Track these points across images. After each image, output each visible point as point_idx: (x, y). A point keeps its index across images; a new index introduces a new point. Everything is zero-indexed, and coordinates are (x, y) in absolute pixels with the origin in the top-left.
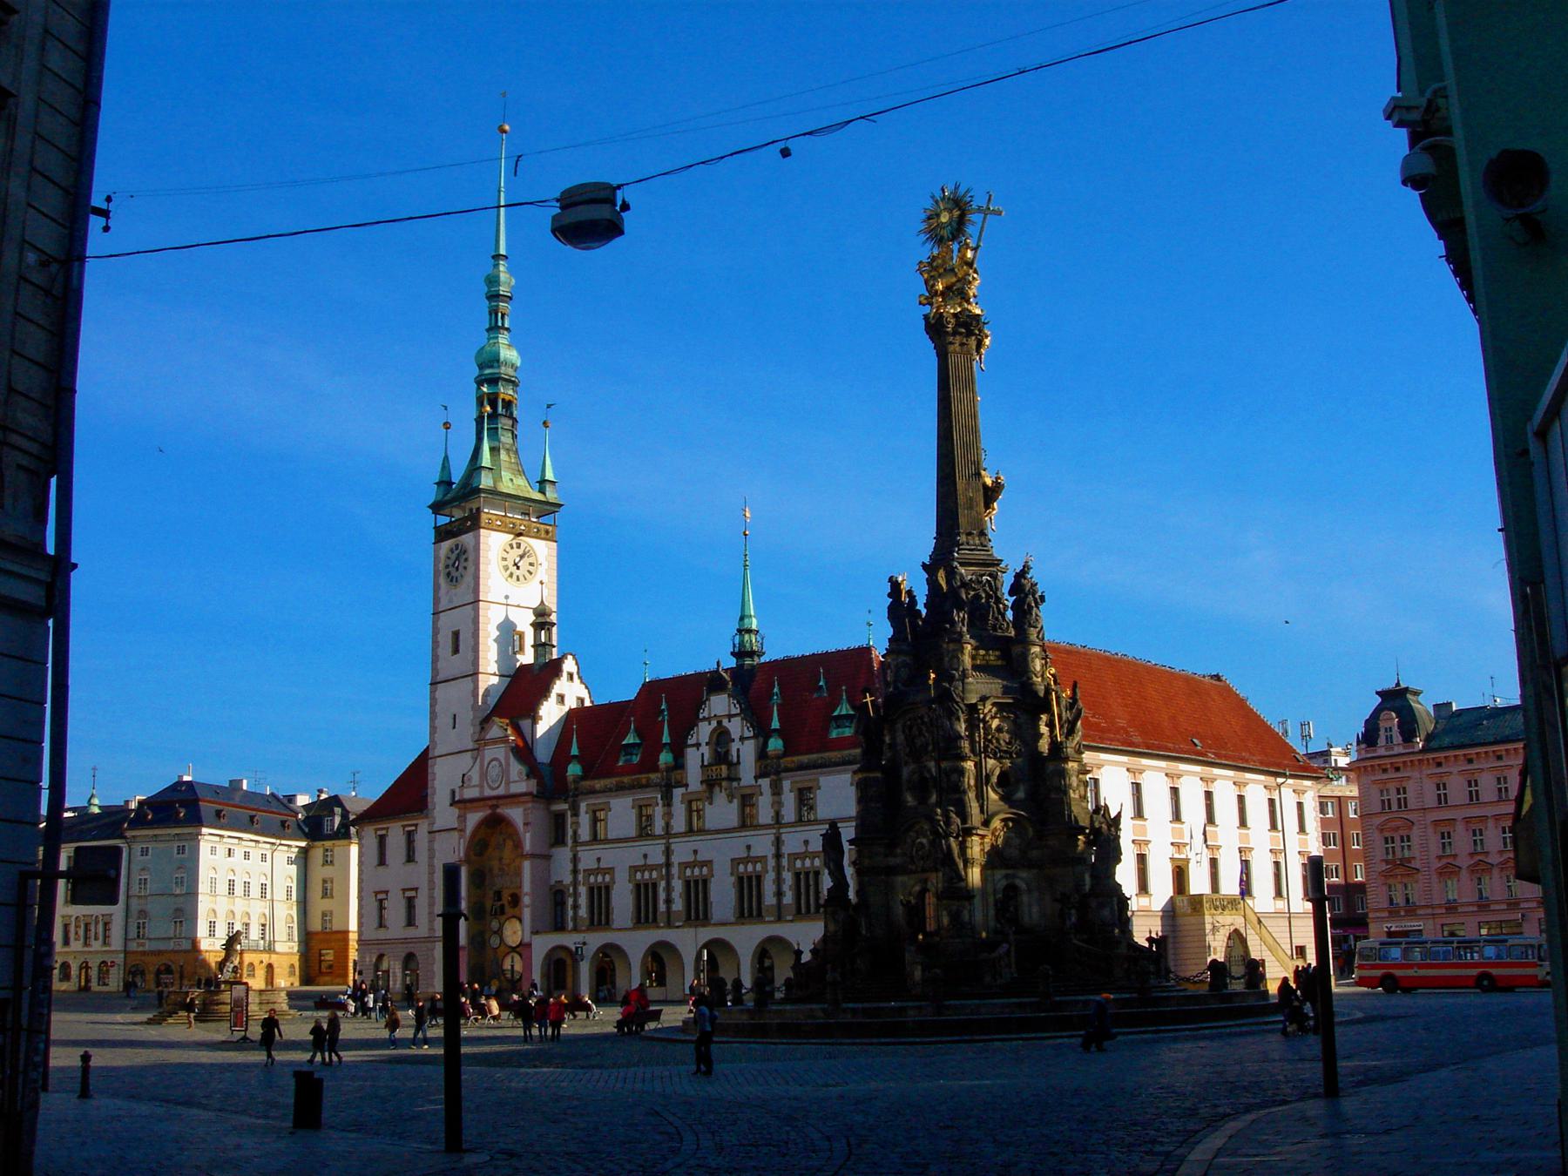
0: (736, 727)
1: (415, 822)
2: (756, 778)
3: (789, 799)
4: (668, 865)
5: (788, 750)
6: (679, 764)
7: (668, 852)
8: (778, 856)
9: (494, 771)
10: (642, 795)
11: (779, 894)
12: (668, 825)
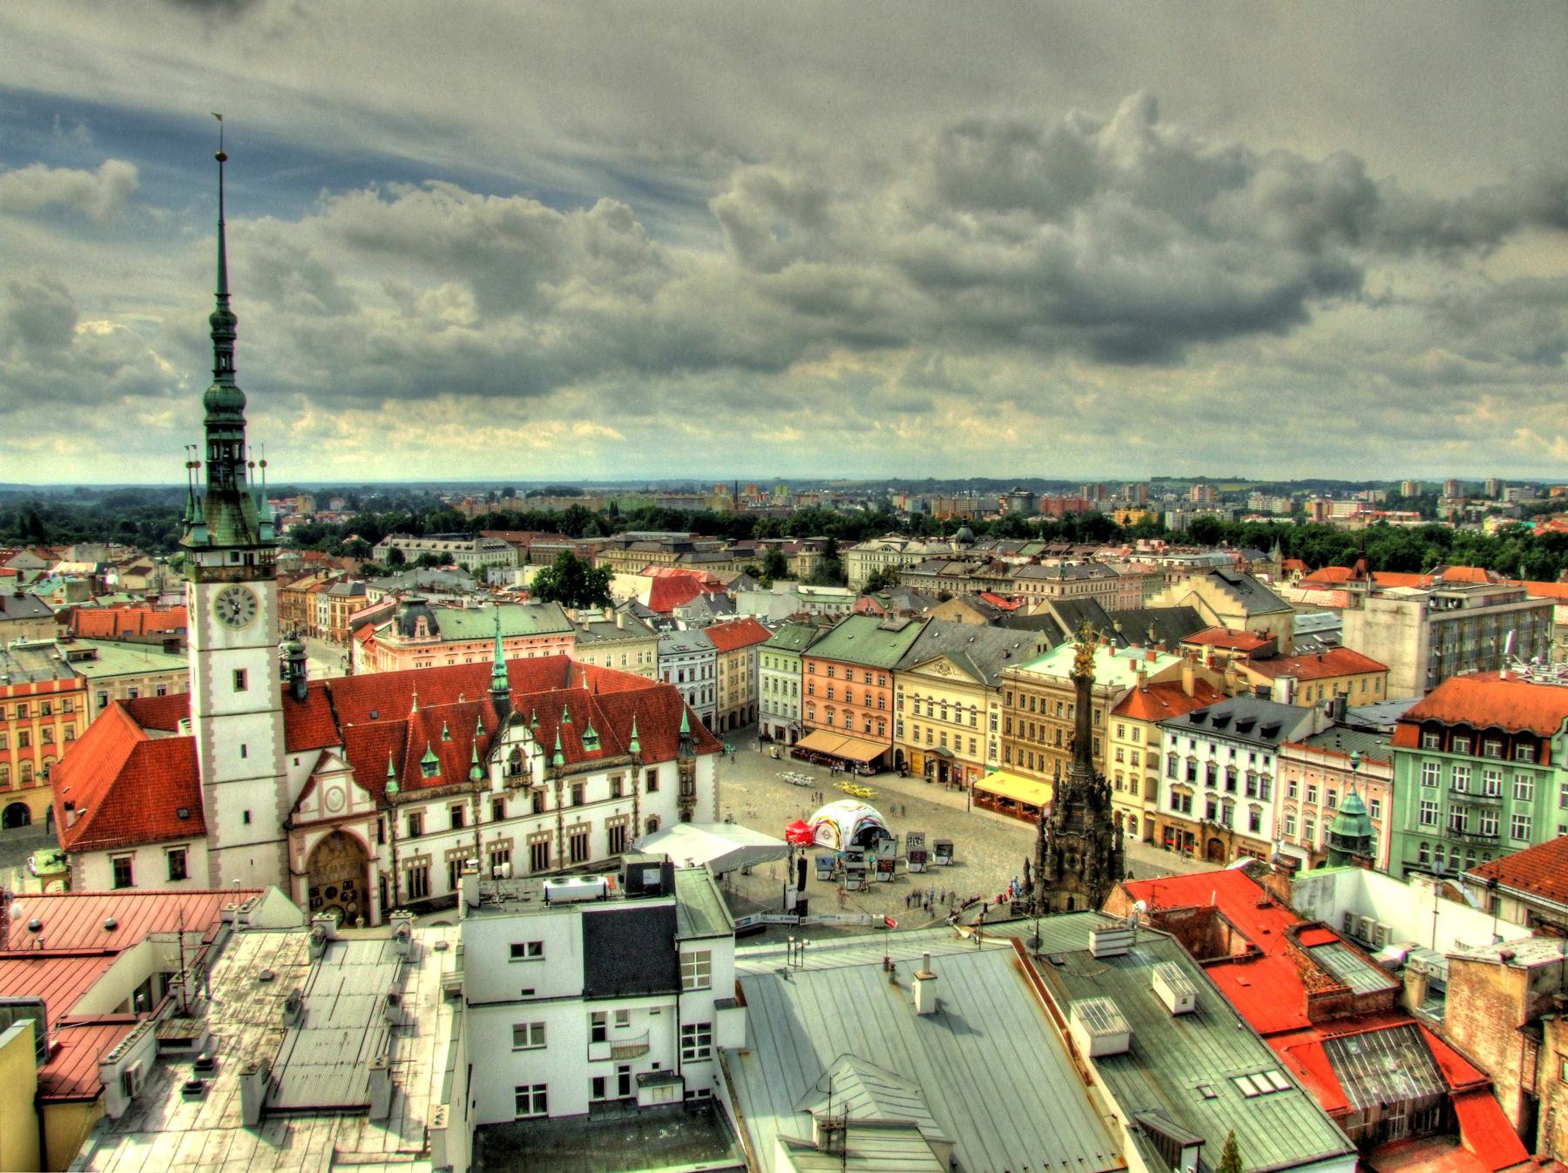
0: (529, 748)
3: (567, 795)
4: (478, 845)
5: (567, 762)
6: (486, 775)
7: (478, 837)
8: (560, 829)
9: (336, 797)
10: (456, 800)
11: (561, 852)
12: (477, 819)
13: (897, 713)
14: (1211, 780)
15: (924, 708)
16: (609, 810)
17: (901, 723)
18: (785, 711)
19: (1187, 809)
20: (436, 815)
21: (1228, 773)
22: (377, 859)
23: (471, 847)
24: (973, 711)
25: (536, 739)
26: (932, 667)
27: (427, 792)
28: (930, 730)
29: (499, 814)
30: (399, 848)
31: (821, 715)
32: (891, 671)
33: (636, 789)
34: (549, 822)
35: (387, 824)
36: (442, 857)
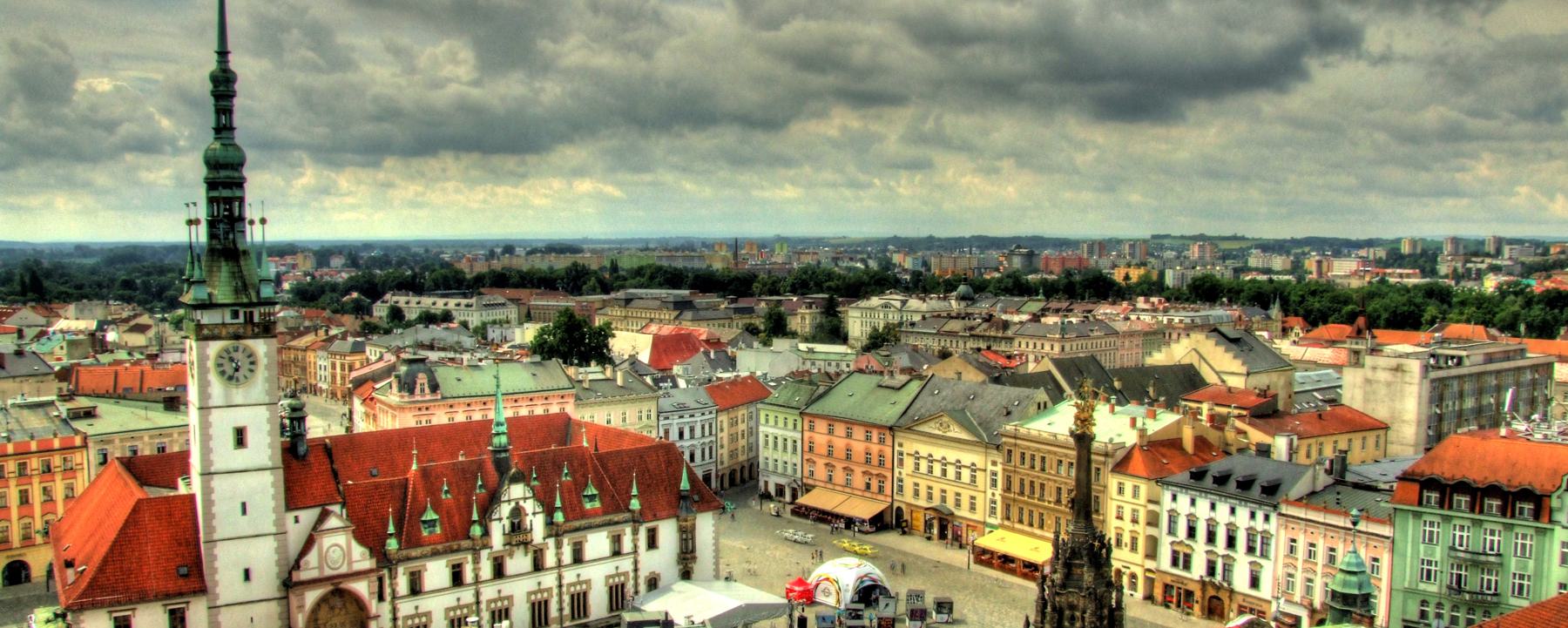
0: (529, 506)
1: (186, 600)
2: (544, 539)
4: (478, 603)
5: (567, 519)
6: (486, 533)
7: (478, 594)
8: (560, 586)
9: (336, 554)
10: (456, 558)
11: (561, 610)
12: (477, 576)
13: (897, 470)
14: (1211, 538)
15: (924, 465)
16: (608, 568)
17: (901, 480)
18: (785, 468)
19: (1187, 566)
20: (436, 572)
21: (1228, 530)
22: (377, 617)
23: (471, 604)
24: (973, 468)
25: (537, 497)
26: (932, 424)
27: (428, 549)
28: (930, 488)
29: (499, 572)
30: (398, 606)
31: (821, 472)
32: (891, 428)
33: (636, 546)
34: (549, 580)
35: (387, 582)
36: (442, 615)
